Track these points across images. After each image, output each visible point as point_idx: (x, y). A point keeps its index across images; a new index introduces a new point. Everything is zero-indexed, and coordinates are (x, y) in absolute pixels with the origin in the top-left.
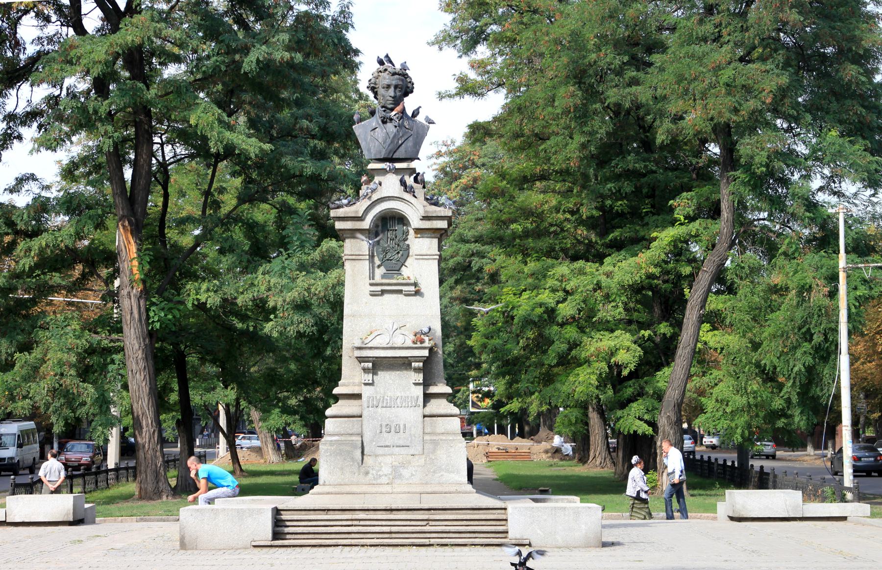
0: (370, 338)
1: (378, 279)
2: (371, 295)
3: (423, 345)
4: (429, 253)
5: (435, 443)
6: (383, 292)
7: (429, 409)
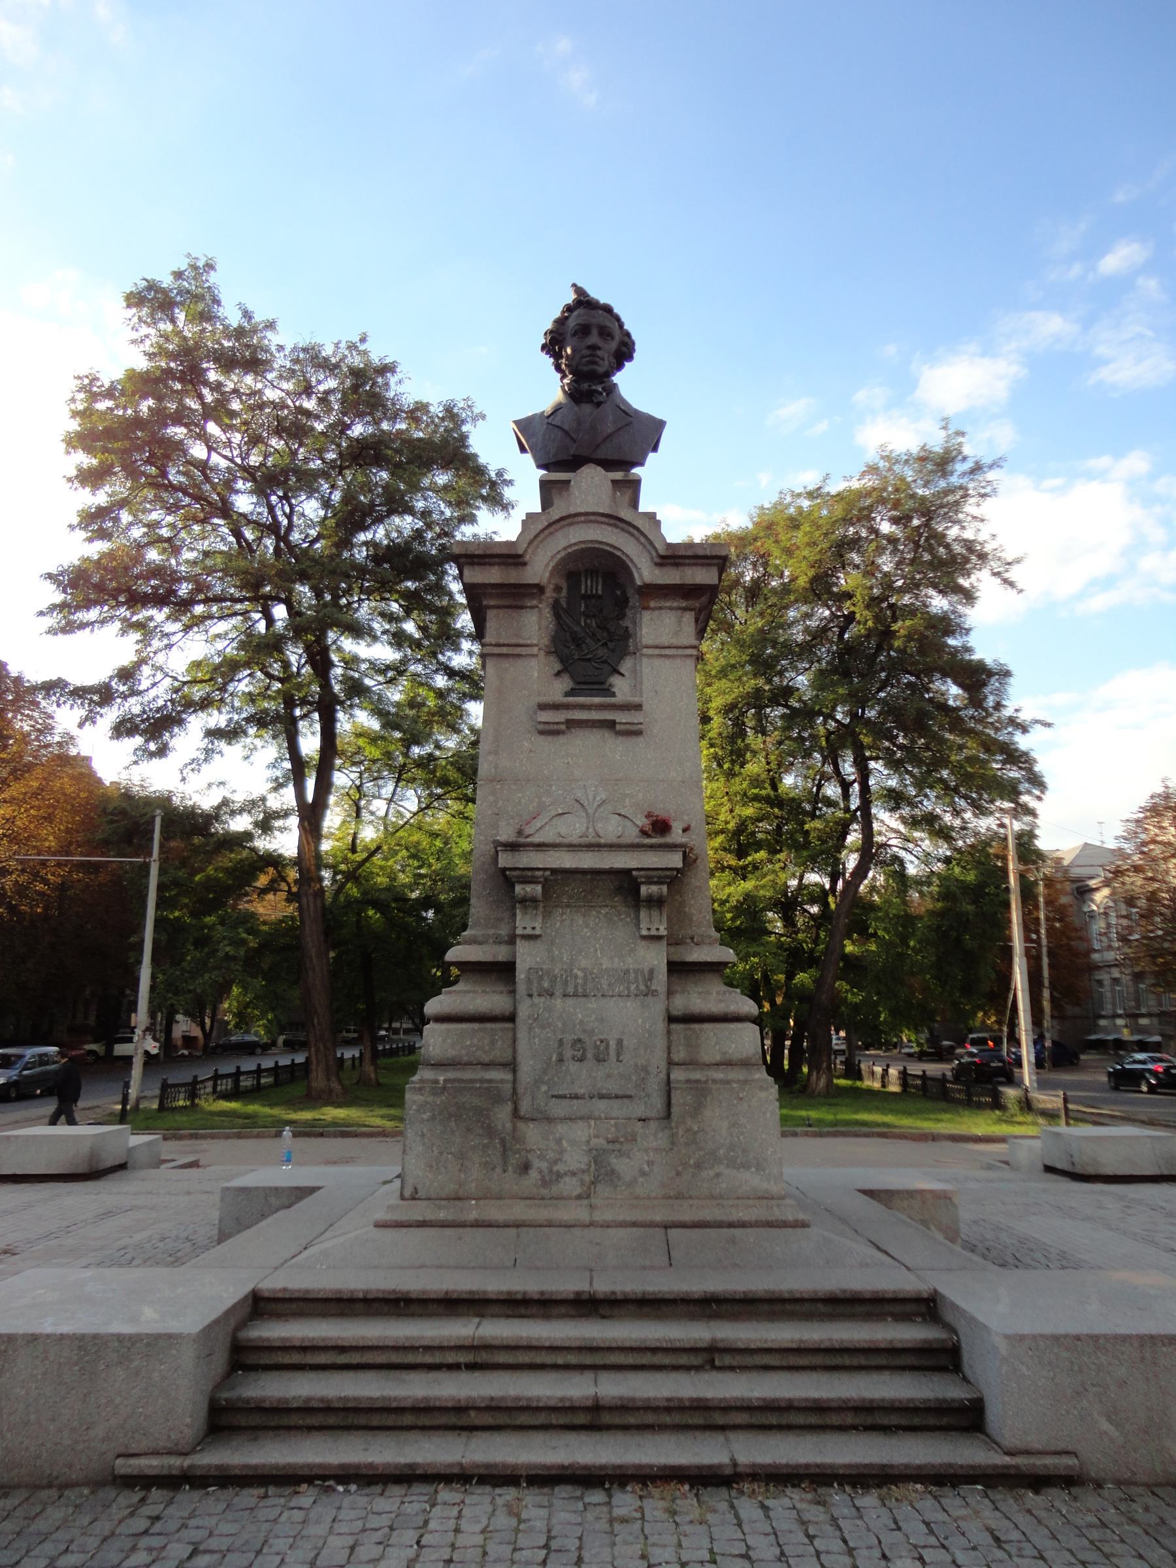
0: (537, 824)
1: (559, 698)
2: (542, 733)
3: (669, 839)
4: (675, 642)
5: (700, 1090)
6: (571, 724)
7: (680, 1004)
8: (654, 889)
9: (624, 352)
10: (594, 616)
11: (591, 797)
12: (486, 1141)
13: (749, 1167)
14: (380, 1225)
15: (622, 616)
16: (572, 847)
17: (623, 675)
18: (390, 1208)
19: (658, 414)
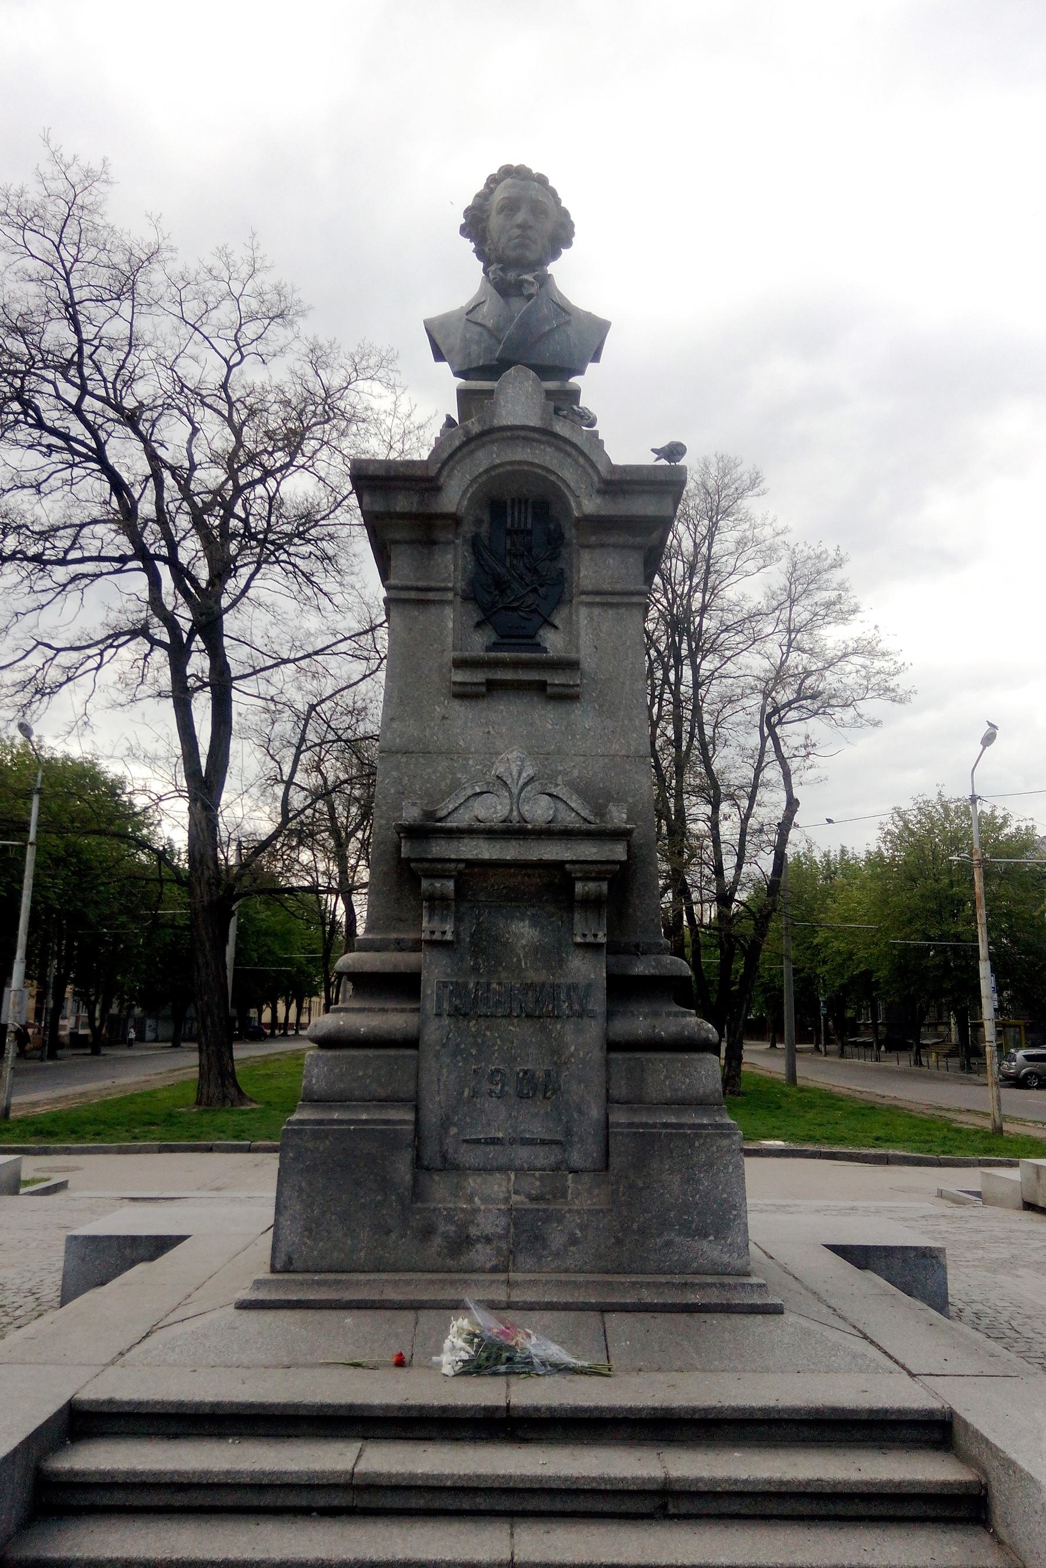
2: (457, 696)
6: (492, 686)
8: (591, 886)
9: (559, 234)
10: (522, 556)
11: (515, 773)
12: (379, 1198)
13: (706, 1236)
14: (244, 1306)
15: (554, 557)
16: (491, 834)
17: (556, 627)
18: (259, 1284)
19: (601, 313)
